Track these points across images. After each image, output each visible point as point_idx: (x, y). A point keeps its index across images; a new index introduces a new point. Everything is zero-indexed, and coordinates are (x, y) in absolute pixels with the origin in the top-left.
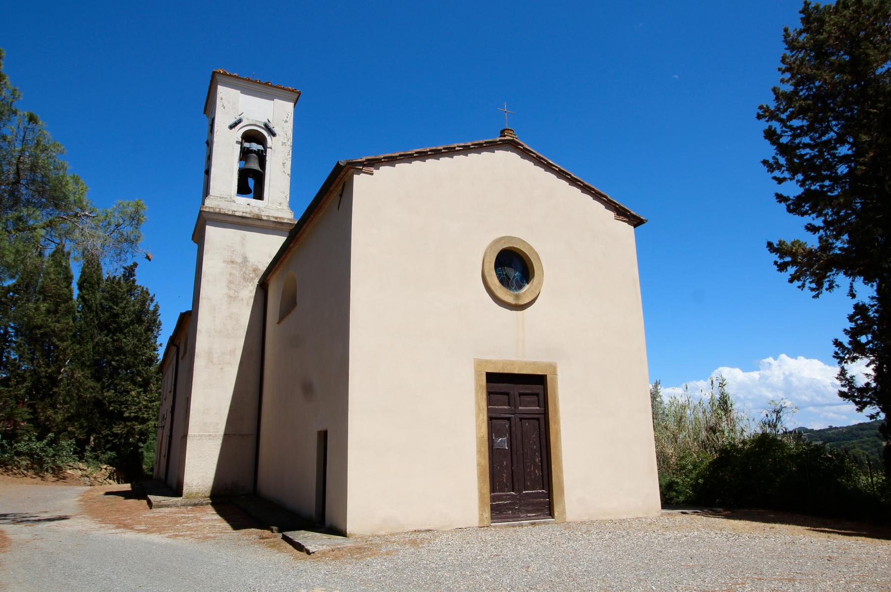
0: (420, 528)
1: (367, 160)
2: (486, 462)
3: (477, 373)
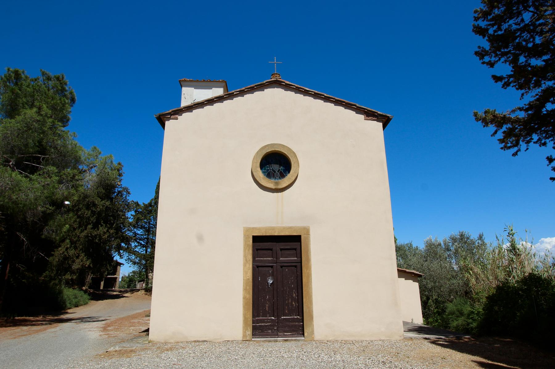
0: (199, 339)
1: (172, 111)
2: (250, 296)
3: (246, 237)
